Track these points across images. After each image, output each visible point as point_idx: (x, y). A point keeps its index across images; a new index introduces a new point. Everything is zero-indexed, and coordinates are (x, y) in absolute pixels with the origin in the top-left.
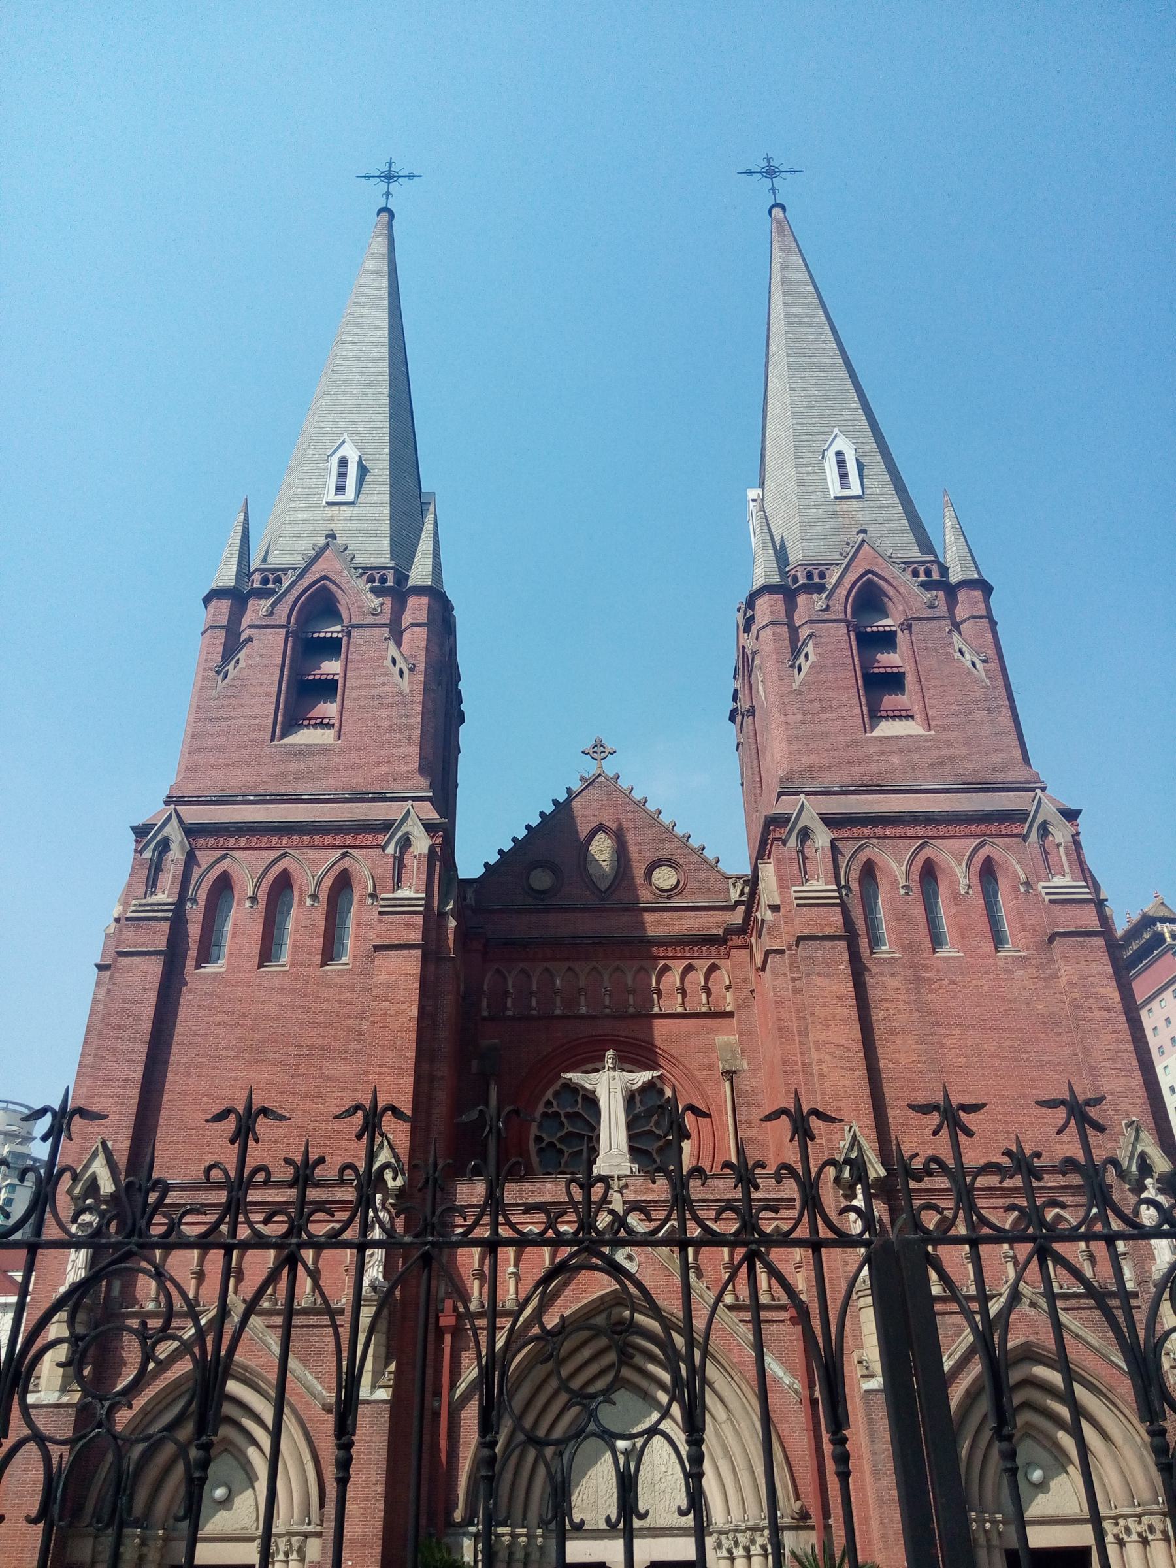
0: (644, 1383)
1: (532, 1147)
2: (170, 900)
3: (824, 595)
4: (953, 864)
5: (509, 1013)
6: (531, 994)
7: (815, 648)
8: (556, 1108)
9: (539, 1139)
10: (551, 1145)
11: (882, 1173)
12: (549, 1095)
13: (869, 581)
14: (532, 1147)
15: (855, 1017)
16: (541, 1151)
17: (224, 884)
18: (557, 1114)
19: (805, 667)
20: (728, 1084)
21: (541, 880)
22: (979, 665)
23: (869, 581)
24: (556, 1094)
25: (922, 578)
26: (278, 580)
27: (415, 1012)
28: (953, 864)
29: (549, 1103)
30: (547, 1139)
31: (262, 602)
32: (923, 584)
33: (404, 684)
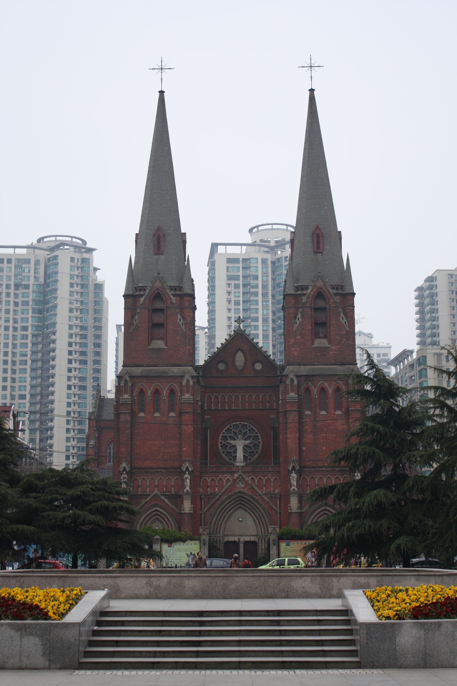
0: (245, 507)
1: (219, 445)
2: (130, 397)
3: (306, 296)
4: (329, 388)
5: (213, 408)
6: (218, 403)
7: (301, 317)
8: (226, 434)
9: (221, 443)
10: (224, 444)
11: (298, 468)
12: (224, 431)
13: (320, 291)
14: (219, 445)
15: (298, 431)
16: (221, 446)
17: (142, 392)
18: (226, 436)
19: (298, 322)
20: (272, 431)
21: (221, 367)
22: (347, 323)
23: (320, 291)
24: (226, 430)
25: (335, 291)
26: (145, 290)
27: (192, 429)
28: (329, 388)
29: (224, 433)
30: (223, 443)
31: (141, 299)
32: (335, 294)
33: (183, 327)
